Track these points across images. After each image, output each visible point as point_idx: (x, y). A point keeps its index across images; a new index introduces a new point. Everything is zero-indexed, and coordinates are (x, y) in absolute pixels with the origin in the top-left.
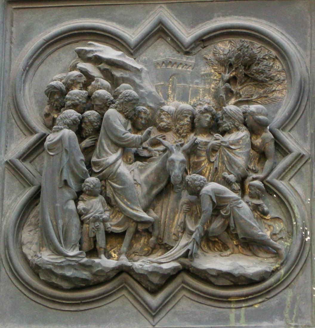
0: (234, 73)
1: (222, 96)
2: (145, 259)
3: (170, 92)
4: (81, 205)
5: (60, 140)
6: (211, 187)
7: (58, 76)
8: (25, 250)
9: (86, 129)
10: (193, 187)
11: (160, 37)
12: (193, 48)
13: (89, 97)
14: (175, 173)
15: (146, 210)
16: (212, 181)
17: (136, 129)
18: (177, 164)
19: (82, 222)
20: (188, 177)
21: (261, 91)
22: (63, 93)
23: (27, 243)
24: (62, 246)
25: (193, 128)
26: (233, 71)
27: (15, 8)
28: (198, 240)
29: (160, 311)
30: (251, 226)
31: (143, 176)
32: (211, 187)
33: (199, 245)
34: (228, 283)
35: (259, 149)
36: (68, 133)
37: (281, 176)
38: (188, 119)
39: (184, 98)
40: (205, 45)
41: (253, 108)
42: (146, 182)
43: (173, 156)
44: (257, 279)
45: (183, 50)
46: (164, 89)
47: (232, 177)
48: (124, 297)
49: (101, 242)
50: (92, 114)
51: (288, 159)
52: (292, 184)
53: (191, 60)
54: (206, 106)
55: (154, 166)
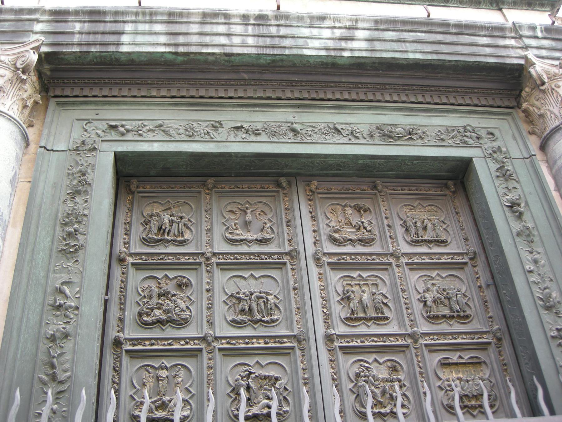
53: (382, 366)
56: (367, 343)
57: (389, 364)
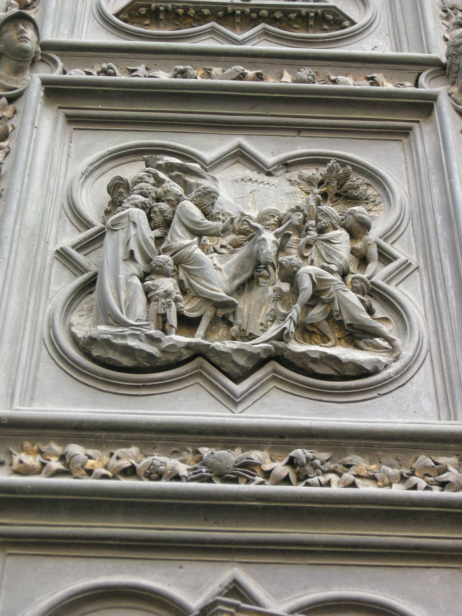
0: (325, 189)
1: (312, 206)
9: (155, 219)
10: (288, 268)
12: (276, 170)
14: (267, 250)
19: (149, 301)
23: (78, 324)
26: (324, 187)
27: (74, 129)
29: (245, 398)
35: (359, 252)
40: (289, 170)
45: (265, 171)
47: (334, 267)
48: (197, 385)
52: (401, 289)
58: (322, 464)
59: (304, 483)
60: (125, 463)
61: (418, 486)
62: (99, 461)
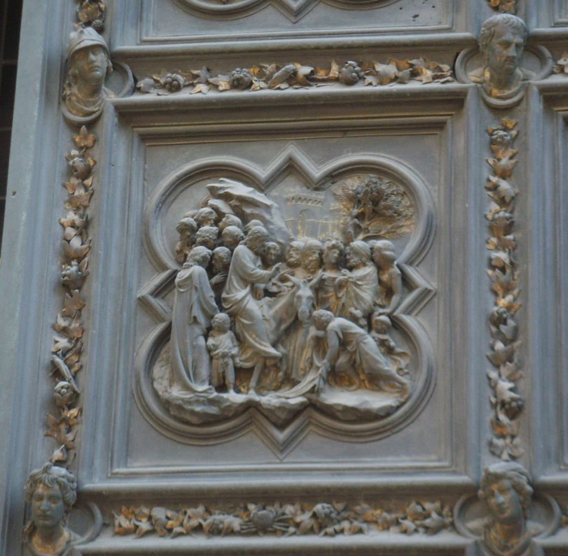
0: (362, 209)
1: (350, 232)
2: (273, 394)
3: (299, 227)
4: (211, 341)
5: (190, 277)
6: (338, 322)
7: (191, 212)
8: (156, 385)
11: (290, 173)
12: (323, 184)
13: (220, 234)
15: (274, 345)
16: (340, 316)
17: (266, 264)
18: (304, 300)
19: (211, 358)
20: (315, 313)
21: (389, 226)
22: (194, 230)
24: (191, 382)
25: (321, 263)
26: (361, 208)
27: (148, 146)
28: (324, 375)
30: (377, 362)
31: (272, 312)
32: (338, 322)
33: (326, 381)
34: (354, 418)
36: (198, 270)
37: (408, 311)
38: (317, 255)
39: (313, 234)
40: (335, 181)
41: (379, 243)
42: (274, 318)
43: (300, 292)
44: (382, 414)
46: (294, 224)
47: (358, 313)
49: (231, 377)
50: (222, 251)
51: (414, 294)
53: (321, 196)
54: (334, 242)
55: (282, 301)
56: (260, 90)
57: (354, 184)
58: (339, 513)
59: (323, 533)
60: (194, 522)
61: (408, 531)
62: (176, 520)
